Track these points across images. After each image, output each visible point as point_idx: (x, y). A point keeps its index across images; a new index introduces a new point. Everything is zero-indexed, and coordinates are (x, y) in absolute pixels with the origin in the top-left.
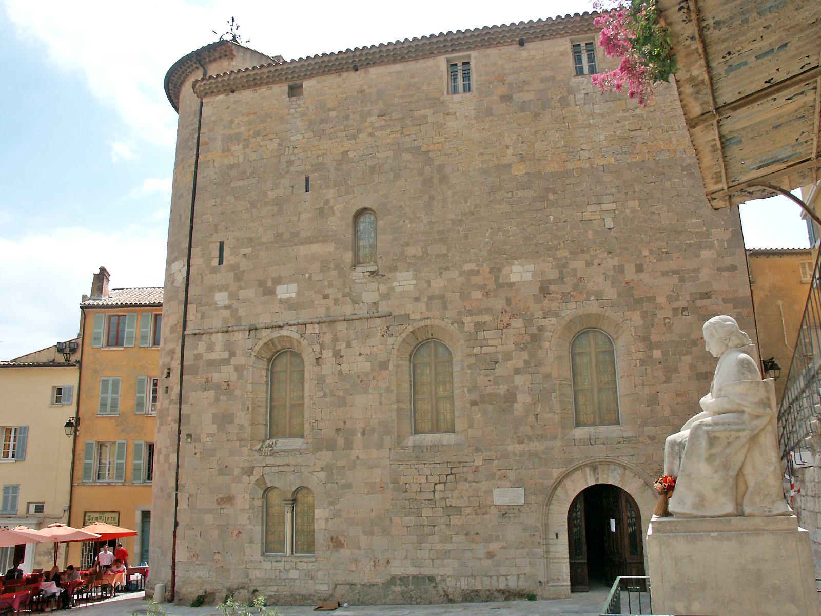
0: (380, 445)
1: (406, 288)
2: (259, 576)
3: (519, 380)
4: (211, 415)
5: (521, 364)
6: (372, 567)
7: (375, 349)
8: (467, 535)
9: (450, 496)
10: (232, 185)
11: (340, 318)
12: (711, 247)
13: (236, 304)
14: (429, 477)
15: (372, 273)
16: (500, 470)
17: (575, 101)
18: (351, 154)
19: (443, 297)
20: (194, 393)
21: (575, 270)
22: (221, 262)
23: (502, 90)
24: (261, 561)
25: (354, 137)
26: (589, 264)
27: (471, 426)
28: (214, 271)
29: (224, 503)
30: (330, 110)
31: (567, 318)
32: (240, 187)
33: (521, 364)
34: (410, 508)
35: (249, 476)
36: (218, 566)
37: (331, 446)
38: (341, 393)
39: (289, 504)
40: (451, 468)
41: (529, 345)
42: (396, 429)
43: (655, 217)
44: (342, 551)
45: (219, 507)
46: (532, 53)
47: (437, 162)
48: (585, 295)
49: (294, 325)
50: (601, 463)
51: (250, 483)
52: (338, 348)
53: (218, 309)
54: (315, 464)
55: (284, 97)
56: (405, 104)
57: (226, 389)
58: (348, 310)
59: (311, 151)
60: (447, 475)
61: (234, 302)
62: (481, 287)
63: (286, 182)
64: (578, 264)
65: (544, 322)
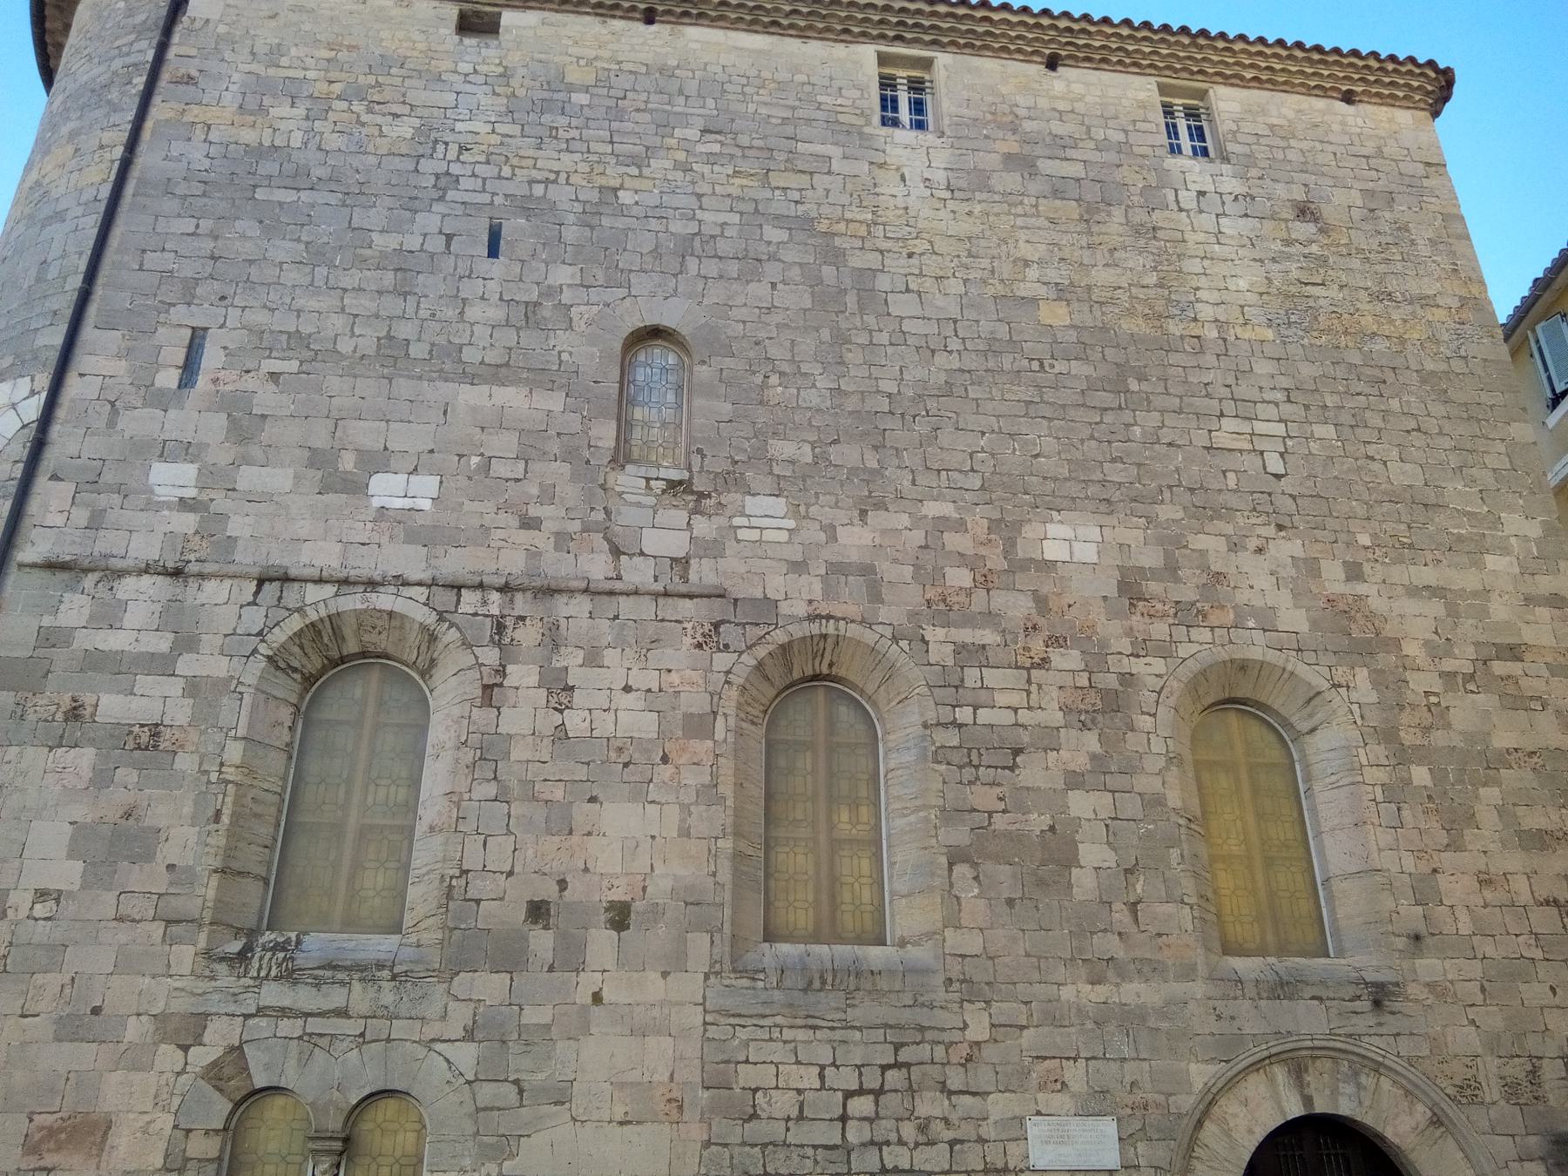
0: (674, 964)
1: (769, 535)
3: (1081, 804)
4: (69, 829)
7: (675, 678)
9: (893, 1137)
10: (260, 194)
11: (575, 584)
12: (1505, 550)
13: (221, 503)
14: (829, 1071)
15: (672, 485)
16: (1045, 1058)
17: (1177, 202)
18: (626, 197)
19: (867, 570)
21: (1203, 553)
25: (638, 162)
26: (1234, 547)
27: (952, 921)
28: (161, 400)
29: (58, 1149)
32: (281, 204)
33: (1081, 762)
35: (185, 1049)
37: (510, 958)
38: (558, 793)
39: (329, 1152)
40: (898, 1047)
41: (1100, 718)
42: (728, 912)
43: (1376, 466)
46: (1078, 88)
47: (856, 261)
48: (1232, 616)
49: (420, 584)
50: (1316, 1053)
51: (183, 1072)
53: (153, 506)
54: (444, 1017)
55: (443, 31)
58: (597, 566)
60: (884, 1068)
61: (218, 495)
63: (429, 221)
64: (1209, 543)
65: (1137, 666)
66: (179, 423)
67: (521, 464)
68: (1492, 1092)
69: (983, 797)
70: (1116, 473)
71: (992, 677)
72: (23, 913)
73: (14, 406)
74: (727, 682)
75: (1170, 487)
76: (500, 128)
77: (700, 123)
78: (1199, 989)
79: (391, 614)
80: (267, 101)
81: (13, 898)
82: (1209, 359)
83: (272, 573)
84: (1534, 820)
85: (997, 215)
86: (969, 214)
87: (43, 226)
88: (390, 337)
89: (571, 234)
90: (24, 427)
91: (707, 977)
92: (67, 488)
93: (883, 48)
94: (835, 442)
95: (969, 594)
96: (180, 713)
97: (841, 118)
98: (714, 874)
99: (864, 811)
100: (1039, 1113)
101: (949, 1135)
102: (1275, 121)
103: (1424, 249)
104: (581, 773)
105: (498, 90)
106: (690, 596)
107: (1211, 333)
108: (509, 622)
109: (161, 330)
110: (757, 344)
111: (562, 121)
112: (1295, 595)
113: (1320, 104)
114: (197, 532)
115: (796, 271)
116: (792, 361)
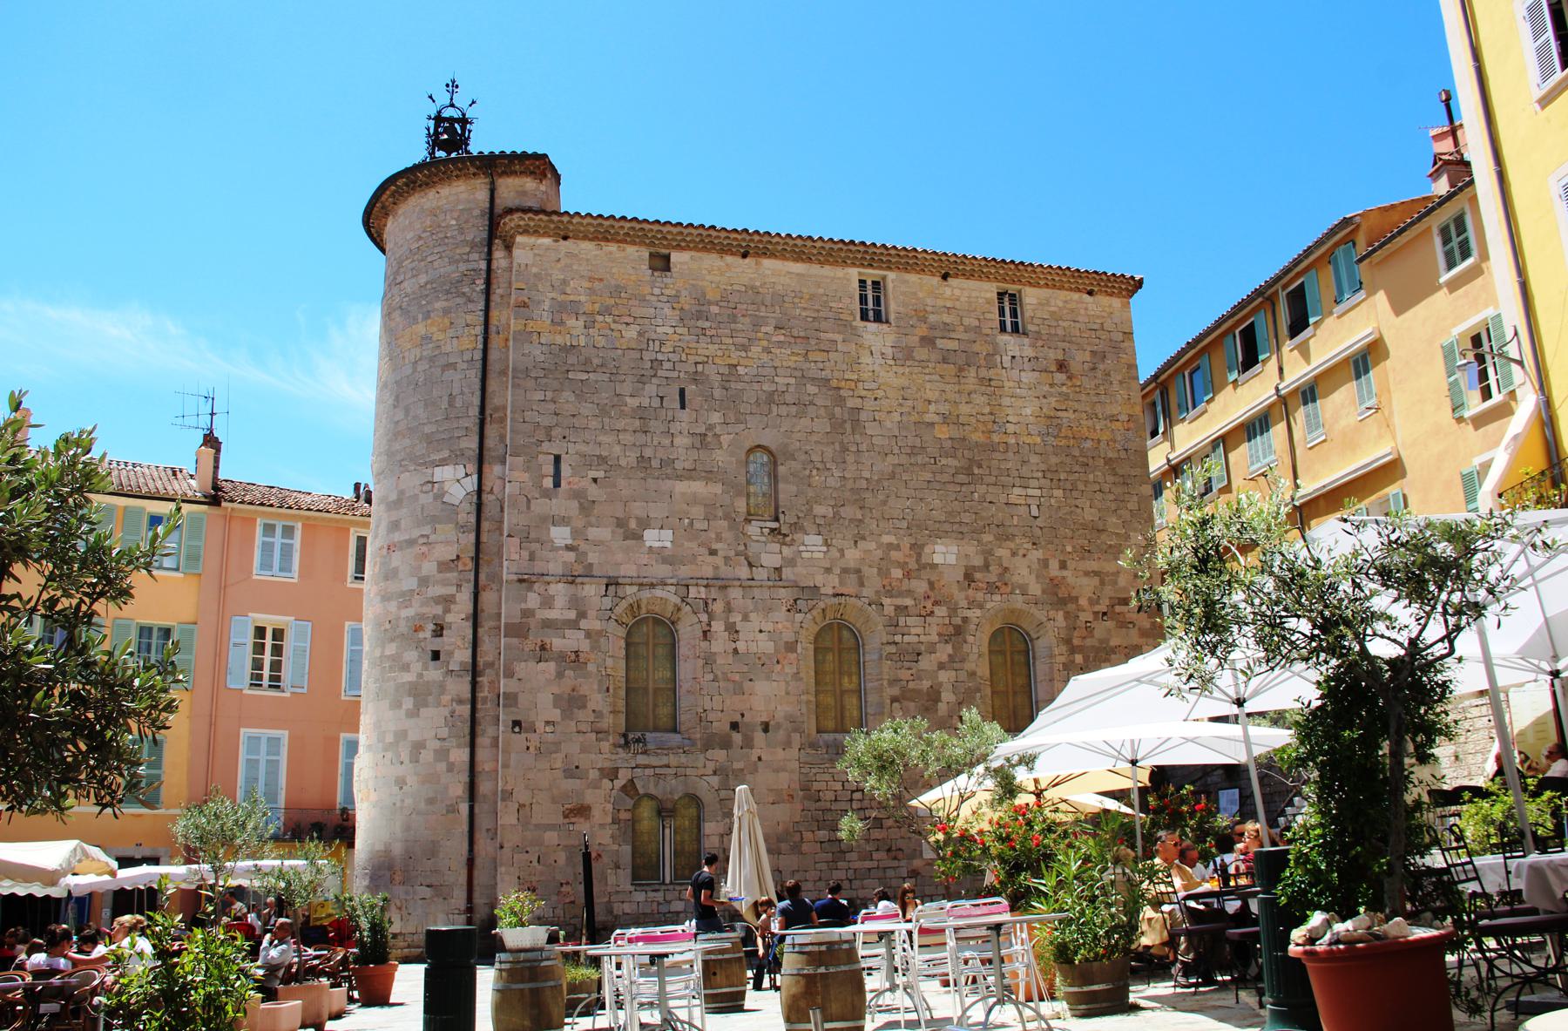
0: (787, 744)
1: (816, 555)
3: (945, 677)
5: (944, 658)
7: (780, 626)
8: (889, 850)
13: (583, 546)
15: (772, 530)
18: (741, 370)
19: (858, 571)
21: (1000, 558)
22: (557, 484)
23: (922, 330)
25: (745, 348)
26: (1014, 554)
28: (546, 494)
30: (710, 303)
33: (944, 658)
37: (726, 744)
38: (737, 677)
43: (1079, 510)
45: (567, 820)
46: (957, 292)
47: (850, 403)
52: (731, 620)
53: (555, 549)
57: (575, 660)
62: (903, 565)
63: (651, 389)
64: (1000, 552)
65: (969, 613)
69: (904, 674)
71: (911, 621)
76: (679, 330)
77: (773, 322)
80: (564, 316)
81: (537, 724)
82: (1010, 454)
87: (443, 371)
88: (642, 457)
89: (717, 393)
92: (516, 541)
95: (901, 581)
96: (585, 646)
97: (841, 316)
99: (855, 678)
102: (1052, 309)
104: (745, 669)
107: (1012, 441)
108: (710, 602)
111: (707, 324)
112: (1037, 577)
113: (1076, 296)
115: (822, 412)
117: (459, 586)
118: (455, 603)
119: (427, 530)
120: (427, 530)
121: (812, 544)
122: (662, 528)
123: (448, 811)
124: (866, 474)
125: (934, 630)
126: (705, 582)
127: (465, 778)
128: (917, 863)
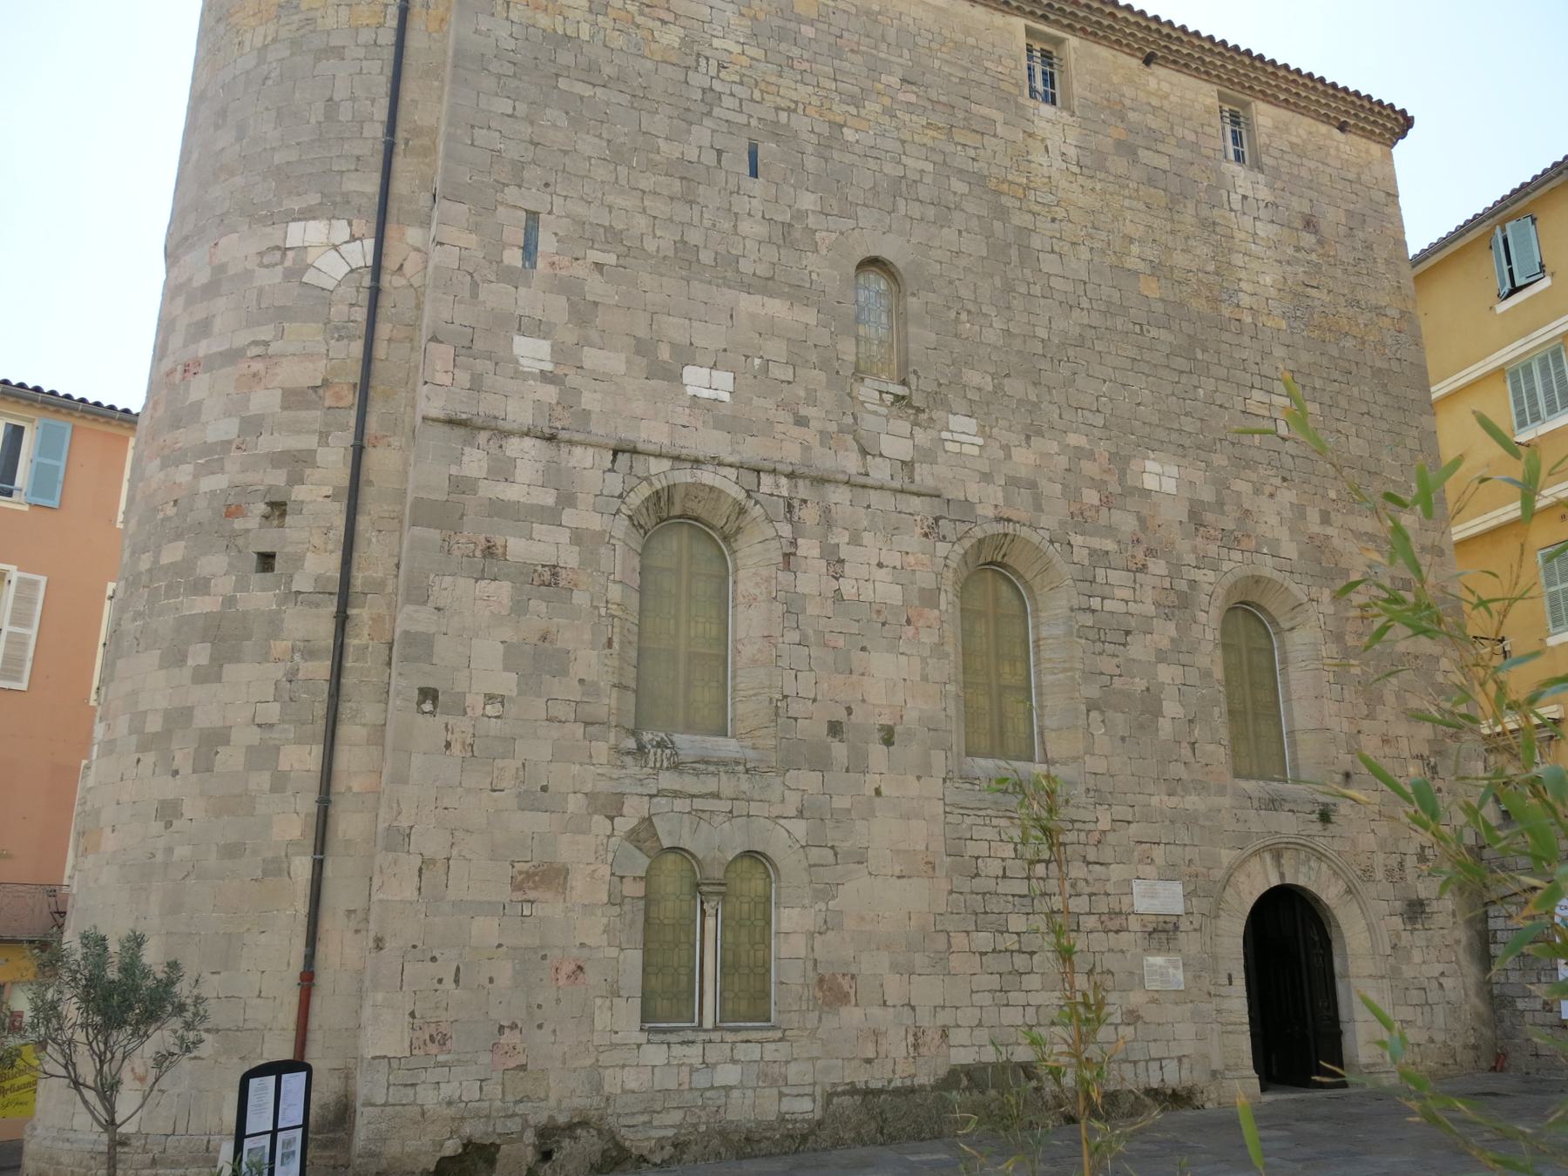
1: (967, 449)
2: (632, 1085)
3: (1166, 673)
5: (1165, 644)
6: (911, 1050)
7: (911, 559)
10: (563, 84)
11: (840, 477)
13: (574, 380)
16: (1141, 843)
19: (1032, 485)
20: (448, 579)
21: (1239, 493)
23: (1118, 132)
24: (639, 1046)
28: (509, 276)
29: (535, 888)
31: (1230, 578)
32: (582, 98)
33: (1165, 644)
34: (986, 913)
36: (511, 1064)
37: (821, 763)
38: (840, 642)
41: (1177, 612)
44: (845, 1011)
45: (519, 896)
46: (1165, 87)
51: (612, 835)
53: (519, 375)
56: (953, 79)
57: (550, 579)
58: (851, 463)
59: (762, 91)
61: (571, 372)
63: (701, 134)
64: (1240, 486)
65: (1198, 575)
66: (529, 299)
67: (791, 371)
68: (1379, 874)
69: (1108, 665)
70: (1189, 425)
71: (1115, 576)
72: (479, 712)
73: (335, 248)
74: (946, 566)
75: (1220, 440)
77: (900, 72)
78: (1226, 801)
79: (712, 488)
81: (469, 700)
82: (1246, 340)
83: (625, 446)
84: (1414, 703)
85: (1111, 194)
86: (1093, 190)
87: (318, 60)
89: (811, 163)
90: (352, 271)
91: (944, 780)
92: (446, 351)
93: (1030, 23)
94: (1007, 375)
96: (570, 558)
97: (1003, 85)
98: (945, 709)
99: (1019, 666)
100: (1138, 878)
101: (1087, 890)
103: (1381, 267)
104: (854, 628)
105: (744, 10)
106: (918, 494)
108: (796, 503)
109: (500, 208)
110: (951, 282)
111: (796, 52)
112: (1291, 530)
113: (1323, 128)
114: (558, 403)
115: (974, 223)
116: (975, 301)
117: (324, 437)
118: (314, 465)
119: (266, 333)
120: (266, 333)
121: (962, 431)
122: (714, 367)
123: (265, 873)
124: (1042, 333)
125: (1149, 596)
126: (790, 469)
127: (309, 804)
128: (1136, 998)
